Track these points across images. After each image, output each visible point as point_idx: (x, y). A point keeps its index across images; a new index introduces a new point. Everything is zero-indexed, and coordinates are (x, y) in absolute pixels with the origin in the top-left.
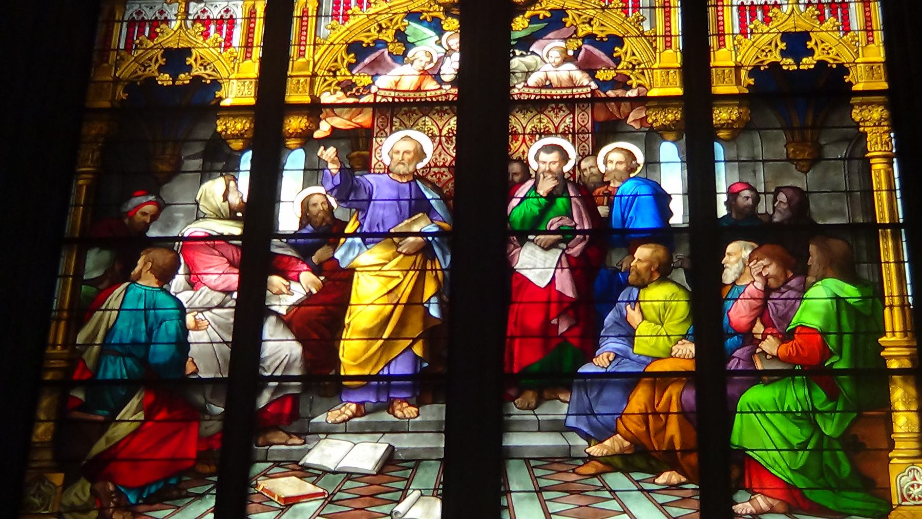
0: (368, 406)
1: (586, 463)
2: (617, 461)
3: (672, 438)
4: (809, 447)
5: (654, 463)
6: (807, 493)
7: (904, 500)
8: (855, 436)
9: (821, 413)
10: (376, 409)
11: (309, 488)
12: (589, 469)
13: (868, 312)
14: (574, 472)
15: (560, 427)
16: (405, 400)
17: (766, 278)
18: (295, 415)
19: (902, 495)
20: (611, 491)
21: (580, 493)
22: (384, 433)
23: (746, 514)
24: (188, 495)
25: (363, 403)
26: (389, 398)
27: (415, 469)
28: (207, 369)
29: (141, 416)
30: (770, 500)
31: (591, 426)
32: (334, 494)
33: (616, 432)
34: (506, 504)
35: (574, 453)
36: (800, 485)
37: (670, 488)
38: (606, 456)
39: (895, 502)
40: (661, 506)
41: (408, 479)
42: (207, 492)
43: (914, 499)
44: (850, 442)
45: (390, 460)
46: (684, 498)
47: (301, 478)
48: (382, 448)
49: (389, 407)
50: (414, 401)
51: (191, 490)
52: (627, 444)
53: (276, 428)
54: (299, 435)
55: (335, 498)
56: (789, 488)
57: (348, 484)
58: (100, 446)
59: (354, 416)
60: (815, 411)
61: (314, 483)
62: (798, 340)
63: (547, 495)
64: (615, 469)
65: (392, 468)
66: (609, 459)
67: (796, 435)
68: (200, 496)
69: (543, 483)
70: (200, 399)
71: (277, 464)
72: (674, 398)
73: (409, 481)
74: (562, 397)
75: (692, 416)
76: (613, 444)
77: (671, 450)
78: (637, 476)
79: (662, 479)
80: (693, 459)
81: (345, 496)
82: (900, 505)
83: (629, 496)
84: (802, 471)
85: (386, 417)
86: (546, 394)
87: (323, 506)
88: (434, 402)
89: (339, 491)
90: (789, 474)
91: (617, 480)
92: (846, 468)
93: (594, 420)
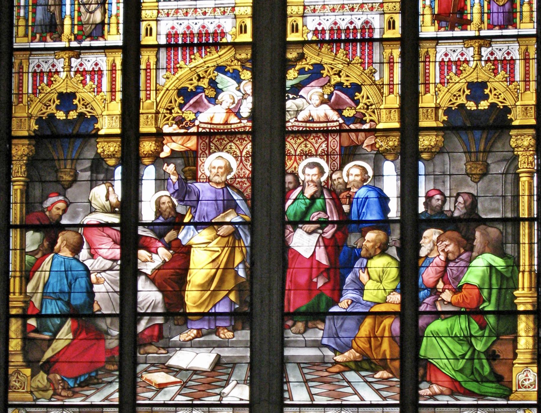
3: (385, 351)
10: (209, 333)
13: (508, 275)
17: (447, 253)
33: (352, 348)
38: (346, 362)
57: (195, 377)
59: (196, 337)
62: (464, 292)
66: (347, 364)
72: (387, 328)
76: (350, 355)
77: (384, 359)
85: (214, 338)
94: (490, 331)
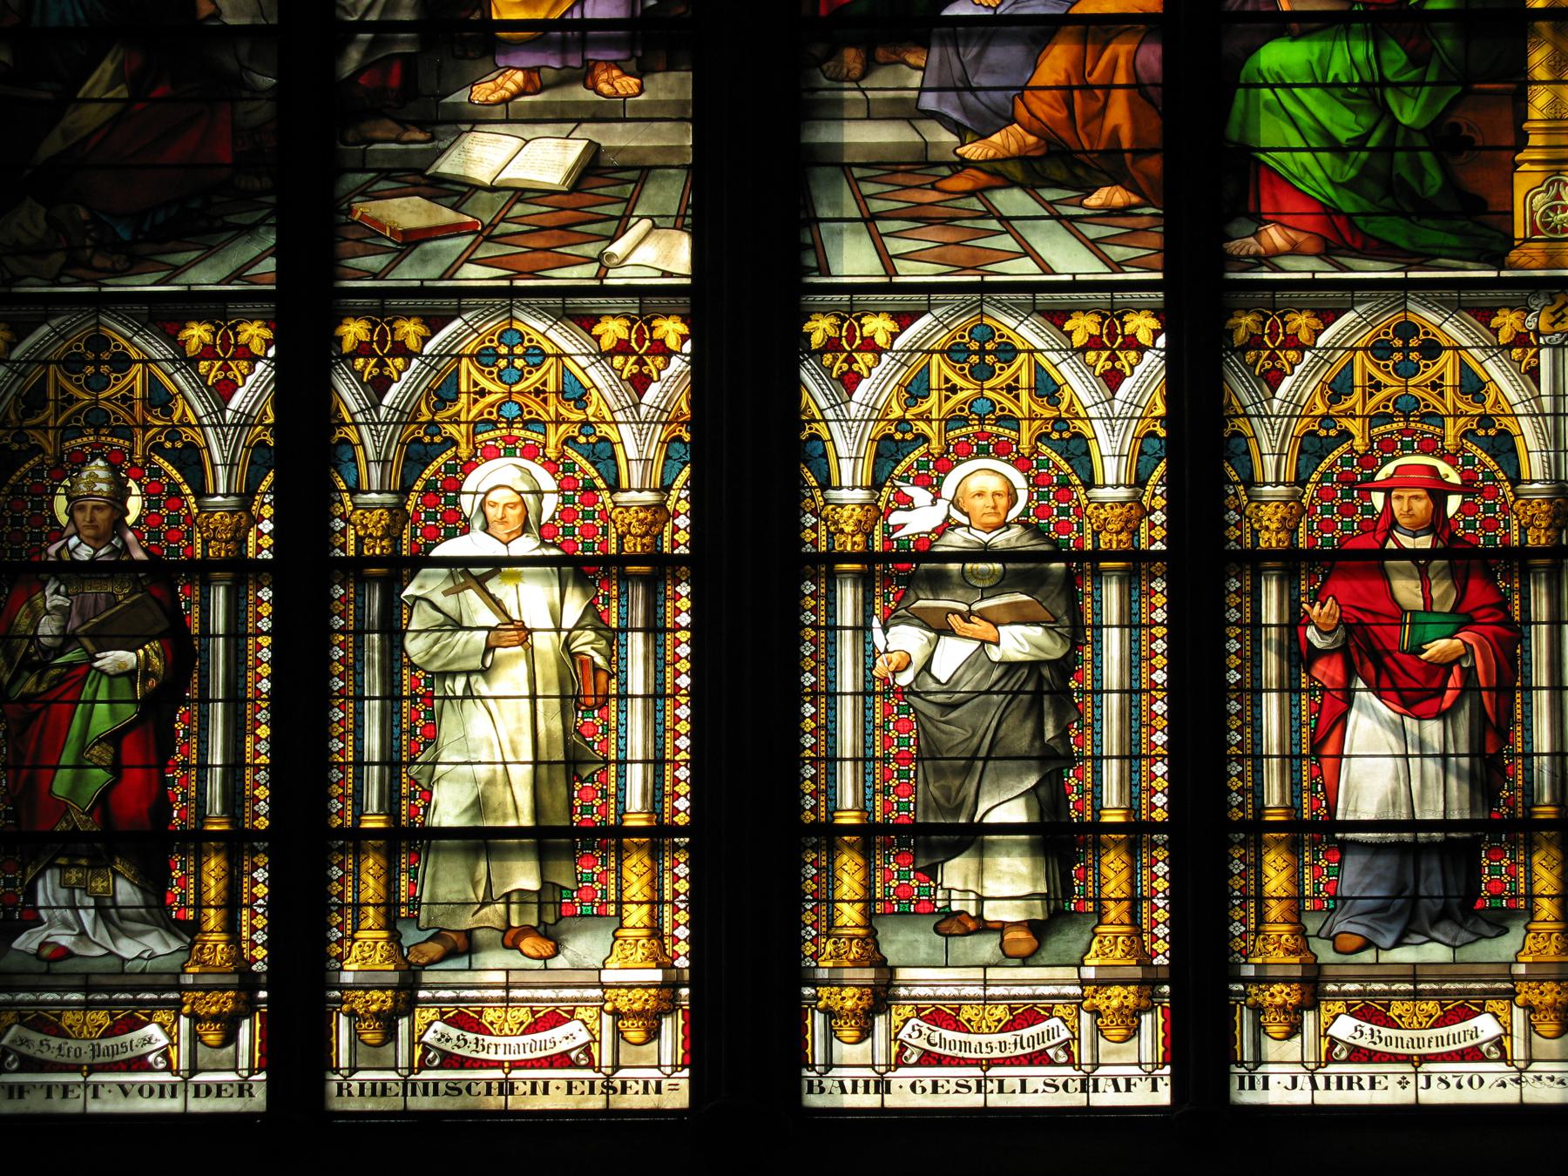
0: (548, 75)
1: (955, 173)
2: (1015, 171)
3: (1116, 129)
4: (1371, 144)
5: (1080, 172)
6: (1360, 221)
7: (1535, 230)
8: (1456, 127)
9: (1397, 86)
10: (562, 82)
11: (447, 216)
12: (961, 183)
14: (934, 188)
15: (910, 113)
16: (616, 64)
18: (410, 90)
19: (1533, 222)
20: (1002, 219)
21: (946, 222)
22: (579, 122)
23: (1248, 256)
24: (227, 227)
25: (537, 69)
26: (585, 62)
27: (640, 183)
28: (236, 10)
29: (122, 92)
30: (1291, 234)
31: (965, 109)
32: (493, 225)
33: (1012, 120)
34: (809, 240)
35: (933, 155)
36: (1348, 206)
37: (1109, 213)
38: (993, 160)
39: (1519, 234)
40: (1093, 245)
41: (628, 201)
42: (262, 222)
43: (1554, 230)
44: (1444, 138)
45: (592, 167)
46: (1135, 230)
47: (429, 198)
48: (576, 149)
49: (585, 76)
50: (632, 65)
51: (233, 219)
52: (1031, 139)
53: (379, 114)
54: (421, 125)
55: (496, 232)
56: (1328, 211)
57: (518, 209)
58: (53, 145)
60: (1384, 83)
61: (455, 208)
63: (883, 226)
64: (1010, 184)
65: (595, 181)
66: (999, 166)
67: (1345, 124)
68: (248, 230)
69: (877, 206)
70: (229, 62)
71: (385, 174)
72: (1122, 62)
73: (631, 203)
74: (912, 59)
75: (1155, 93)
76: (1006, 140)
78: (1049, 195)
79: (1095, 200)
80: (1154, 165)
81: (514, 228)
82: (1526, 240)
83: (1034, 228)
84: (1351, 185)
85: (582, 94)
86: (881, 54)
87: (474, 246)
88: (670, 68)
89: (503, 220)
90: (1330, 191)
91: (1012, 201)
92: (1434, 178)
93: (969, 98)
94: (1443, 68)
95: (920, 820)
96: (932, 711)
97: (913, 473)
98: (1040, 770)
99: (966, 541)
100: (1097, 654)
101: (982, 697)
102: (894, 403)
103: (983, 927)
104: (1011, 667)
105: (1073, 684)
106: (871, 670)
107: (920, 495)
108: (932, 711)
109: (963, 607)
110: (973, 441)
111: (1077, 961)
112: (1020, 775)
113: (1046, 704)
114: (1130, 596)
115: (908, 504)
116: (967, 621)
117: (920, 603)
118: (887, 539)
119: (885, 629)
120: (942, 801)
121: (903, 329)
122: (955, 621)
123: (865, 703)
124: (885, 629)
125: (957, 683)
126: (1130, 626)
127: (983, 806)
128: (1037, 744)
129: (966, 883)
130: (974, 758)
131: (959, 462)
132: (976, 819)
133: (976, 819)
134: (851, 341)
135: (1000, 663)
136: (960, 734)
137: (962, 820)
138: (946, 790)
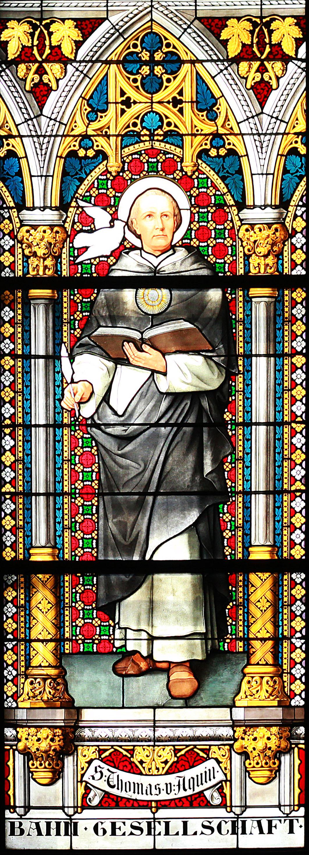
95: (101, 558)
96: (111, 444)
97: (94, 192)
98: (200, 506)
99: (140, 265)
100: (248, 384)
101: (152, 429)
102: (78, 117)
103: (154, 668)
104: (177, 398)
105: (227, 416)
106: (60, 400)
107: (100, 216)
108: (111, 444)
109: (136, 335)
110: (144, 158)
111: (229, 702)
112: (184, 509)
113: (205, 437)
114: (275, 323)
115: (88, 225)
116: (141, 350)
117: (101, 331)
118: (72, 264)
119: (72, 358)
120: (119, 537)
121: (85, 37)
122: (130, 349)
123: (55, 435)
124: (72, 358)
125: (131, 415)
126: (275, 356)
127: (153, 544)
128: (197, 478)
129: (139, 622)
130: (145, 493)
131: (133, 181)
132: (147, 557)
133: (147, 557)
134: (41, 49)
135: (168, 394)
136: (134, 468)
137: (136, 558)
138: (122, 526)
